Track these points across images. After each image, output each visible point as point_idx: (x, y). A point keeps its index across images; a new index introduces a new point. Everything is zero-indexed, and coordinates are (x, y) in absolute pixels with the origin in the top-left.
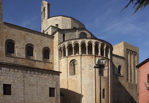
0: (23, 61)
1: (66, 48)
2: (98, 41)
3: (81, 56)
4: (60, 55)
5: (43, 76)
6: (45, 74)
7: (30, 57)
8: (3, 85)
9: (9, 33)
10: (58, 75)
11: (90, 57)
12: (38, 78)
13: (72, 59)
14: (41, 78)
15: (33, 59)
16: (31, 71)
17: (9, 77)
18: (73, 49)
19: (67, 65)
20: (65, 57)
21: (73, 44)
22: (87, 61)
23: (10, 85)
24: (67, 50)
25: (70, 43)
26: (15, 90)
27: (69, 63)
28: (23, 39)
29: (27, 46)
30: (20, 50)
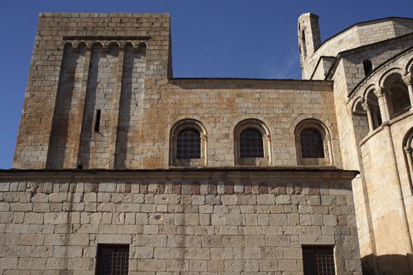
1: (379, 95)
5: (270, 198)
6: (276, 190)
7: (252, 159)
8: (96, 248)
10: (340, 187)
14: (259, 209)
15: (263, 165)
16: (216, 185)
17: (122, 215)
20: (380, 127)
21: (402, 72)
23: (125, 248)
24: (382, 103)
26: (141, 266)
27: (401, 146)
28: (227, 109)
30: (218, 145)
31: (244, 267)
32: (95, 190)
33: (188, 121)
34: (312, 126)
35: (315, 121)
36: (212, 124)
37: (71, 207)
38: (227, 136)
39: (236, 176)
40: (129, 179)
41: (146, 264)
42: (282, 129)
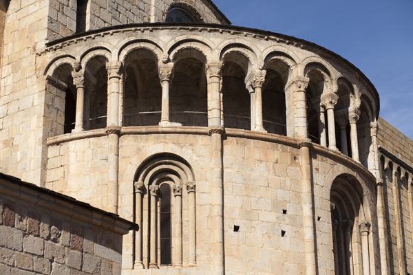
1: (113, 72)
2: (324, 62)
3: (224, 136)
4: (53, 115)
6: (26, 222)
11: (277, 152)
13: (153, 146)
18: (165, 87)
19: (112, 186)
20: (102, 131)
22: (260, 172)
24: (115, 89)
25: (143, 45)
27: (132, 178)
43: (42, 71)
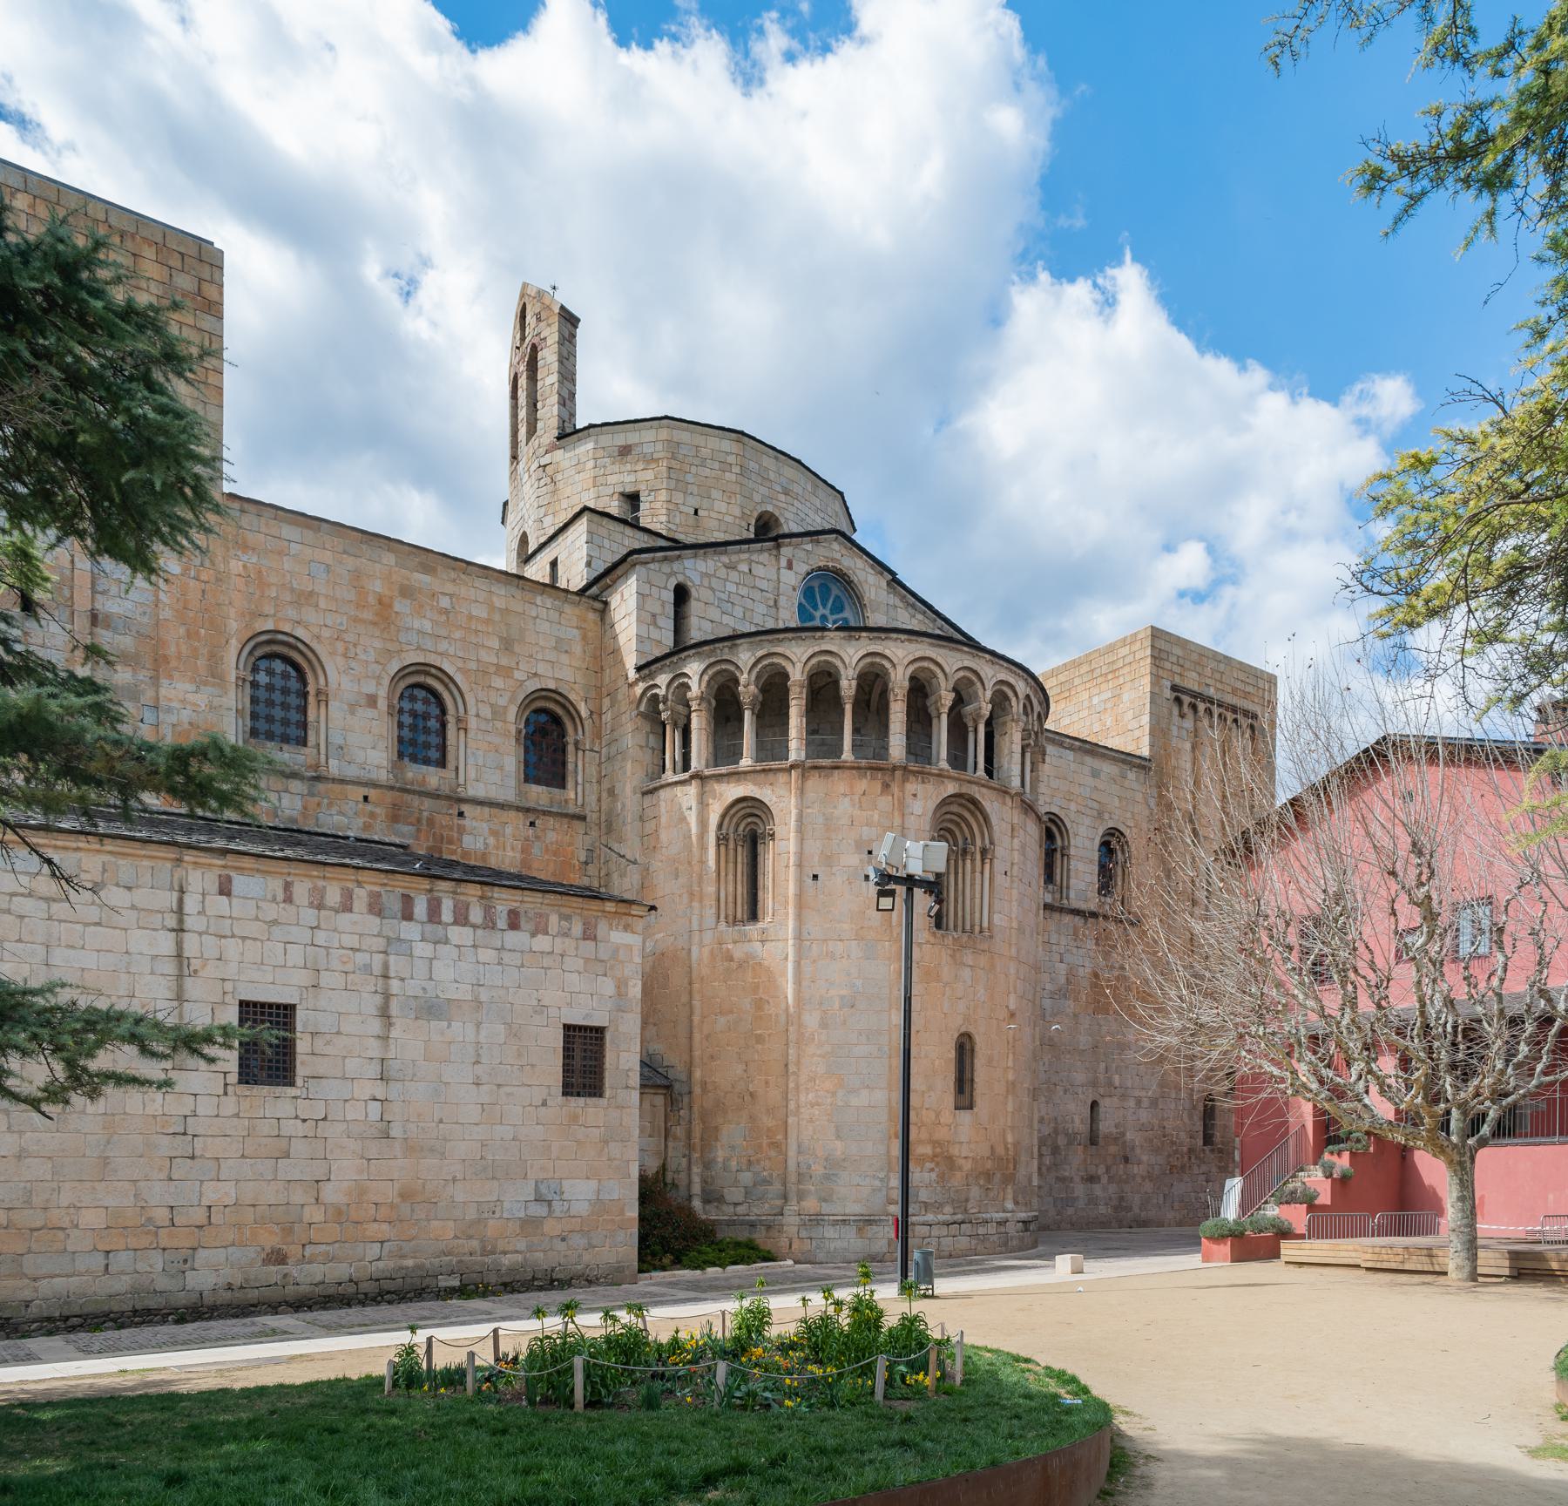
0: (369, 807)
9: (269, 585)
12: (487, 955)
13: (734, 791)
21: (743, 679)
29: (402, 685)
31: (479, 1055)
32: (225, 890)
33: (280, 637)
34: (551, 706)
35: (558, 697)
36: (340, 660)
37: (181, 921)
38: (372, 701)
39: (472, 892)
40: (289, 874)
41: (328, 1043)
42: (492, 705)
43: (634, 706)
